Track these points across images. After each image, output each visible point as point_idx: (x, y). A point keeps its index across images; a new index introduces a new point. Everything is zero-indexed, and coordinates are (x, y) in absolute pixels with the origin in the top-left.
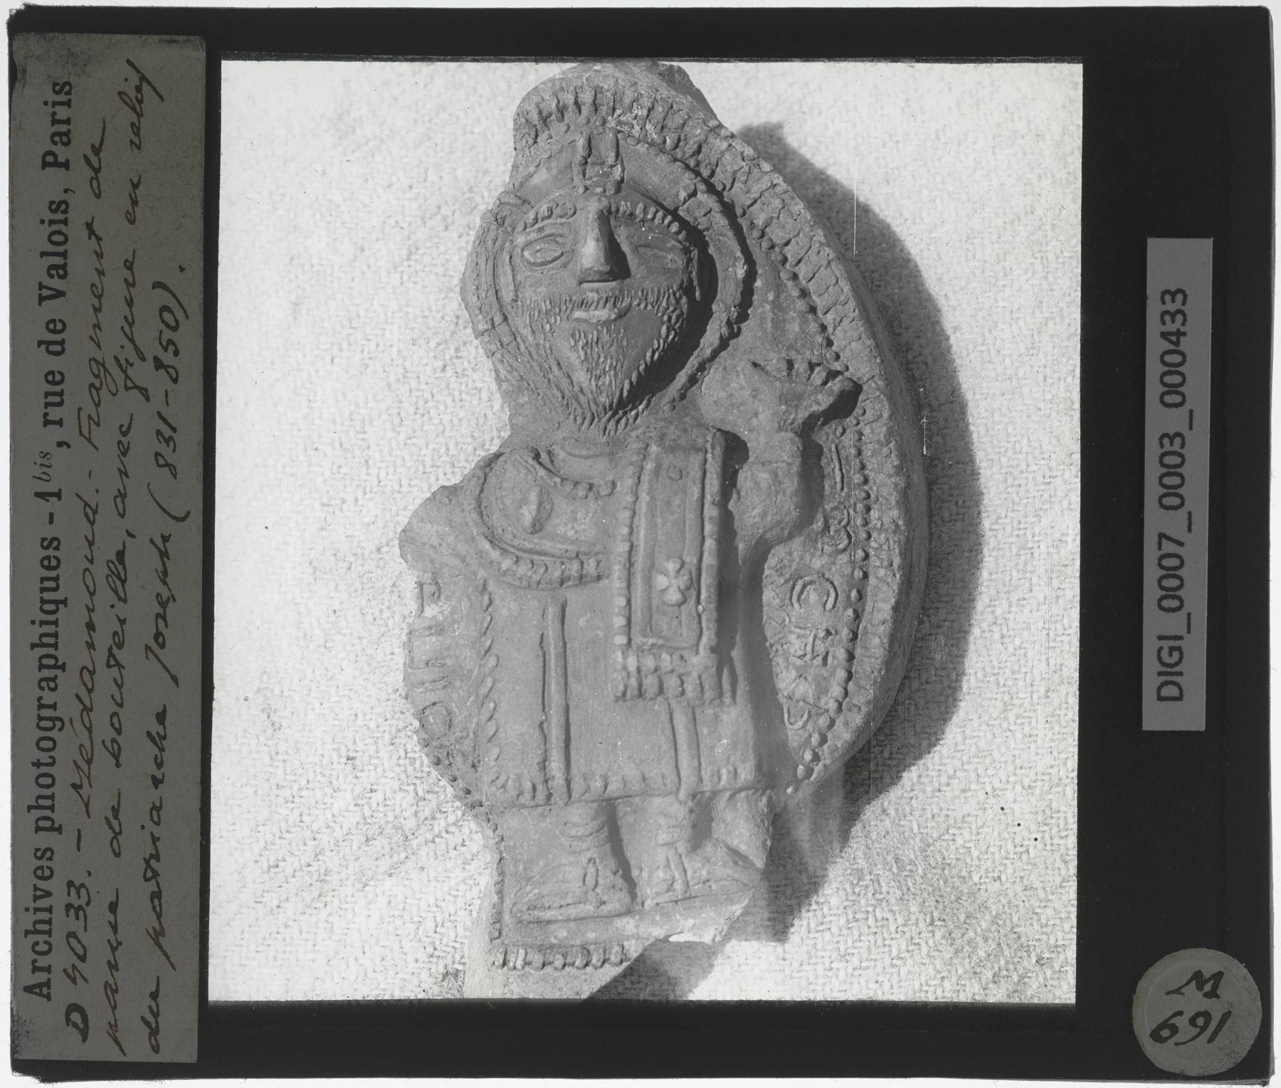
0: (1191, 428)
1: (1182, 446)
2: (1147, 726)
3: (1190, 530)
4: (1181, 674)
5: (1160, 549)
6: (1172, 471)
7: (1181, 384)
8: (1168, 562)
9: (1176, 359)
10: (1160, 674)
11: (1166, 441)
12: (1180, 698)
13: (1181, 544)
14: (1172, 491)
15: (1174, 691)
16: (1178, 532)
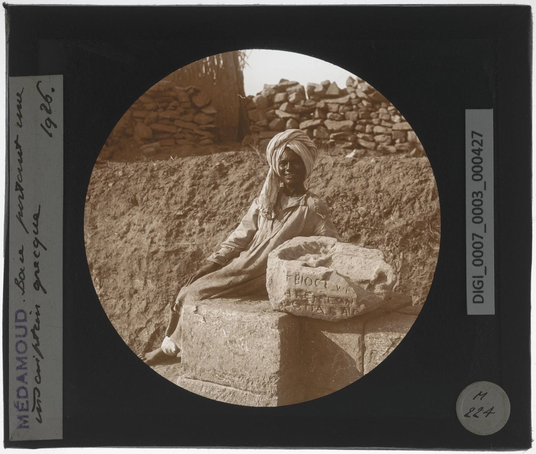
0: (485, 189)
1: (482, 197)
2: (469, 313)
3: (485, 231)
4: (482, 292)
5: (473, 239)
6: (478, 207)
7: (481, 171)
8: (477, 245)
9: (478, 161)
10: (474, 292)
11: (475, 195)
12: (482, 302)
13: (482, 238)
14: (478, 216)
15: (480, 299)
16: (481, 233)
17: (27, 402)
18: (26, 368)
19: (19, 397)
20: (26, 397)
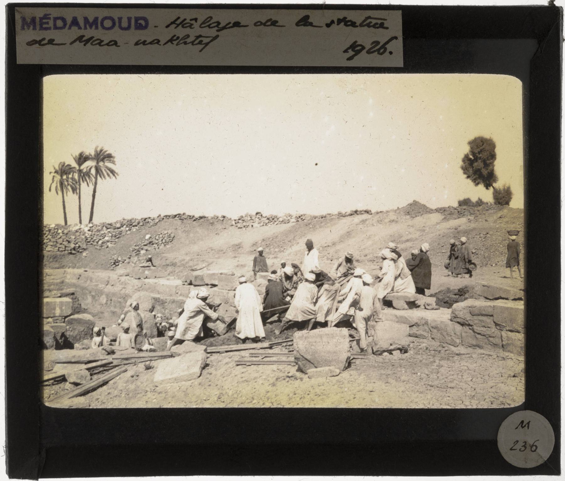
17: (49, 29)
18: (86, 28)
19: (56, 19)
20: (56, 28)
